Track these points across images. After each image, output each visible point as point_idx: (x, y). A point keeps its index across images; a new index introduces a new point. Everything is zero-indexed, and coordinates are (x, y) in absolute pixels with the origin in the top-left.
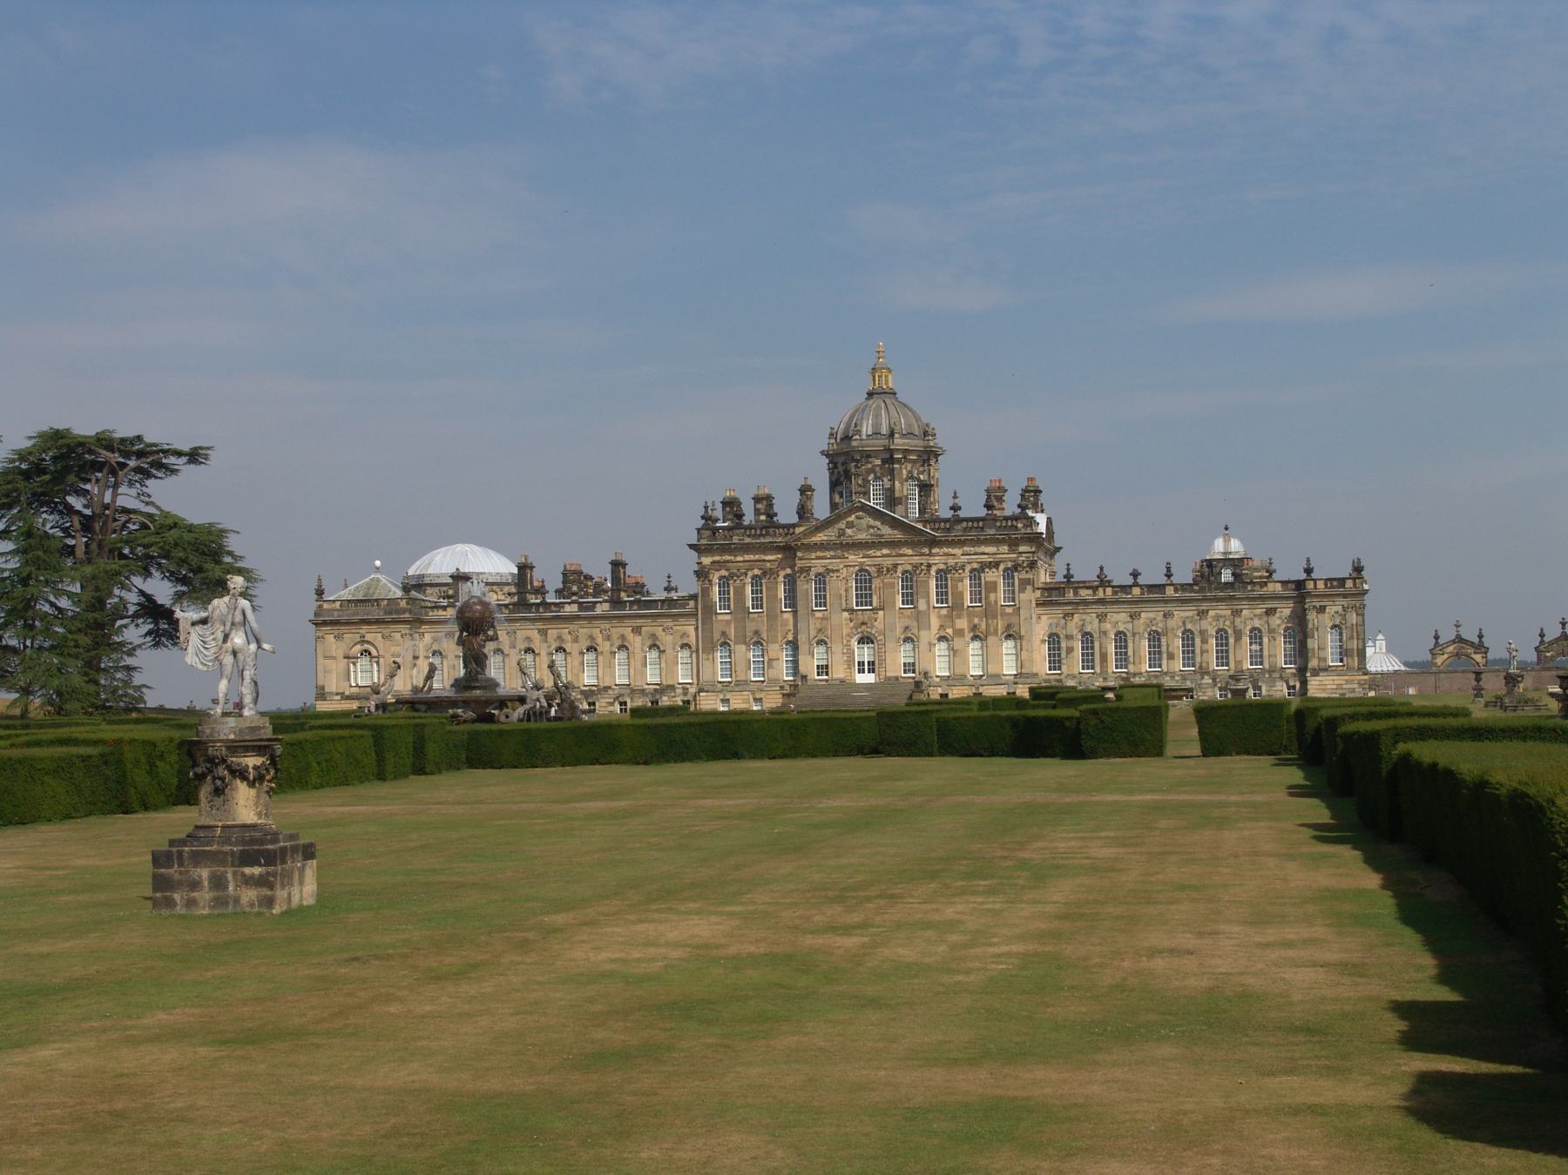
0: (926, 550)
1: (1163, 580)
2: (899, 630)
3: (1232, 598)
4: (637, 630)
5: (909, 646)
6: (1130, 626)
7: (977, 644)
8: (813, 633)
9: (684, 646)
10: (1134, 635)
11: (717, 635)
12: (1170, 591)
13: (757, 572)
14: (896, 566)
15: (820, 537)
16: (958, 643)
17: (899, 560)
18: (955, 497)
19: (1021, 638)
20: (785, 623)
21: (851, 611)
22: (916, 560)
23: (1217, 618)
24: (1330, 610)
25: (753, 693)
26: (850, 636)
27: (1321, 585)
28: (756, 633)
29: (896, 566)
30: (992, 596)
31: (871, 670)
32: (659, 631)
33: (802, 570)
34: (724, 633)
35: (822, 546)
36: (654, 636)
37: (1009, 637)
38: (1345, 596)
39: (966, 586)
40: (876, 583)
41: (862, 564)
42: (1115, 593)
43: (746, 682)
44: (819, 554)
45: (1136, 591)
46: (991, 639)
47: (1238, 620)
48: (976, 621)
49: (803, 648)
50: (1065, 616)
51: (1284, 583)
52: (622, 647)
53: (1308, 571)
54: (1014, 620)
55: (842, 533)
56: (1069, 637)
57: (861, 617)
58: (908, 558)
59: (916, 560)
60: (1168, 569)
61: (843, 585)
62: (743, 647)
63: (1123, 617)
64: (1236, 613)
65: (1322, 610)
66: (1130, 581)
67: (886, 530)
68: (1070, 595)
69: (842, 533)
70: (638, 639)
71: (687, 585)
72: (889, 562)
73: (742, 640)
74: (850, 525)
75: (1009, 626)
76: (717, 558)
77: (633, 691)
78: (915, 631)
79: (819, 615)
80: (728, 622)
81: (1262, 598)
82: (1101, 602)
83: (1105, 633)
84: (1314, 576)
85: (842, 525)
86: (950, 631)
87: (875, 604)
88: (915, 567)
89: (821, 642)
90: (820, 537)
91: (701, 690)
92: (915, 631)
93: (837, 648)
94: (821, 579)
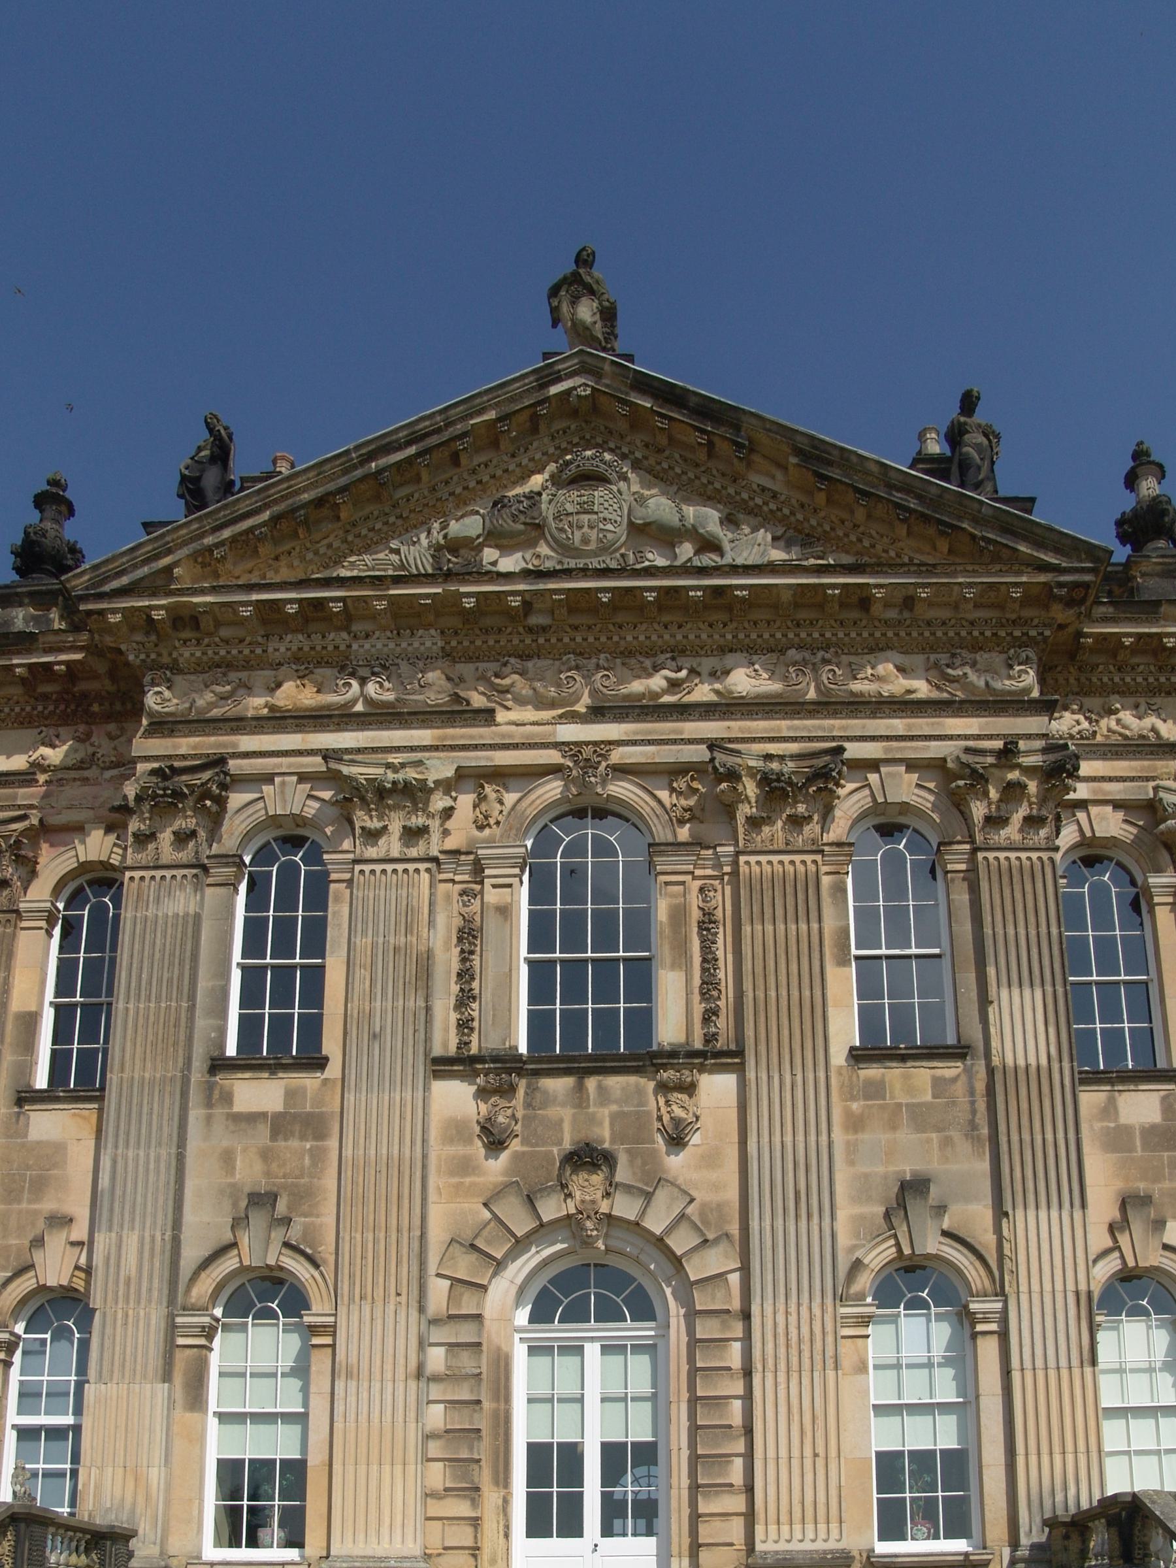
2: (851, 1213)
5: (920, 1334)
26: (482, 1252)
29: (824, 773)
40: (676, 895)
44: (295, 694)
49: (129, 1324)
55: (457, 561)
61: (438, 923)
79: (259, 1094)
85: (469, 526)
87: (672, 1024)
89: (267, 1293)
92: (976, 1215)
93: (378, 1333)
94: (291, 873)
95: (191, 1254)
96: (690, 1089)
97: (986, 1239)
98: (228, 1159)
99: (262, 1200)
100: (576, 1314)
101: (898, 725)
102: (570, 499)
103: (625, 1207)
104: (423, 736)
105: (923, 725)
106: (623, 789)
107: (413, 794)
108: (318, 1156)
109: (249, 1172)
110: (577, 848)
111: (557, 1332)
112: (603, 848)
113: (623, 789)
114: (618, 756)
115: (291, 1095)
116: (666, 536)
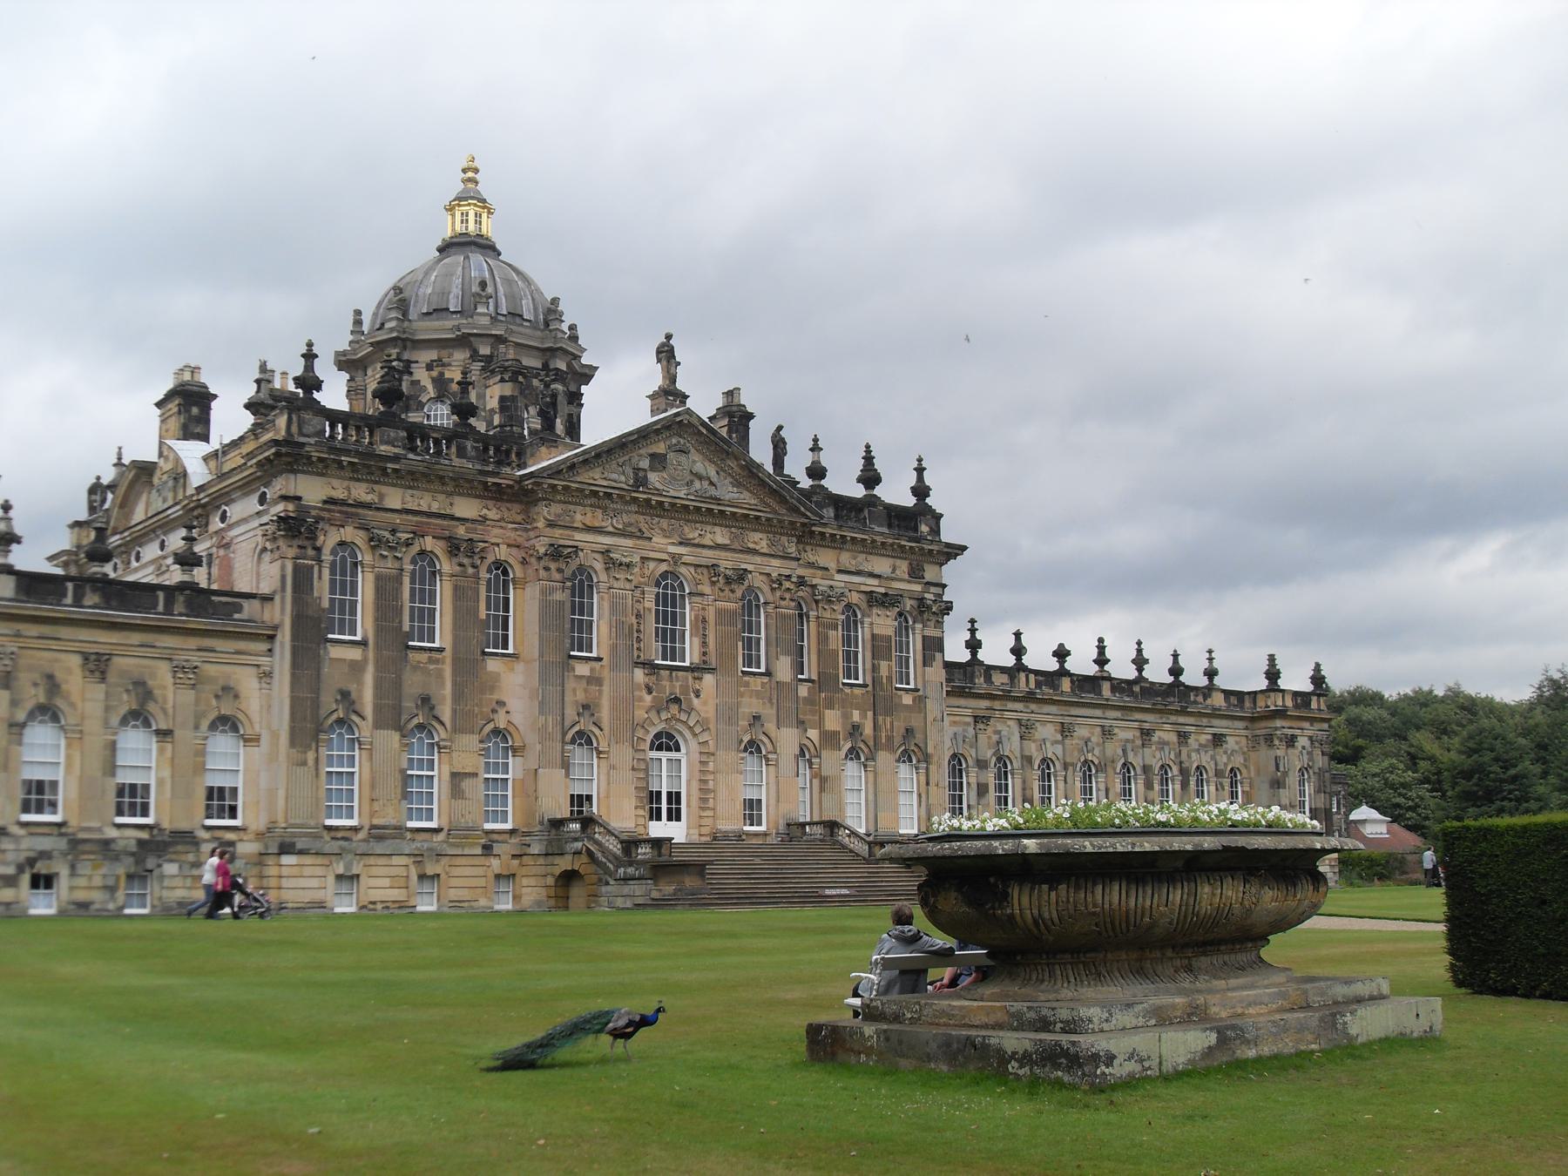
0: (792, 549)
1: (1092, 670)
3: (1183, 712)
4: (97, 665)
5: (751, 763)
6: (1059, 749)
7: (852, 768)
8: (571, 713)
9: (227, 723)
10: (1066, 766)
11: (328, 701)
12: (1106, 686)
13: (429, 543)
14: (742, 575)
15: (595, 477)
16: (831, 760)
17: (749, 562)
18: (816, 448)
19: (927, 758)
20: (492, 684)
21: (650, 667)
22: (776, 567)
23: (1163, 744)
24: (1303, 741)
25: (418, 857)
27: (1289, 703)
28: (426, 701)
30: (884, 664)
31: (674, 815)
32: (162, 677)
33: (556, 553)
34: (345, 695)
35: (600, 498)
36: (143, 690)
37: (906, 757)
38: (1312, 720)
39: (835, 638)
41: (676, 558)
42: (1038, 684)
43: (399, 831)
45: (1066, 684)
46: (884, 758)
47: (1184, 751)
48: (856, 716)
50: (976, 719)
51: (1228, 694)
52: (47, 712)
53: (1273, 675)
54: (916, 722)
56: (982, 764)
57: (669, 686)
58: (765, 562)
59: (776, 567)
60: (1101, 648)
62: (396, 736)
63: (1047, 732)
64: (1183, 737)
65: (1291, 741)
66: (1052, 665)
67: (727, 491)
68: (980, 681)
69: (640, 481)
70: (98, 691)
71: (248, 560)
72: (727, 562)
73: (389, 717)
74: (658, 461)
75: (909, 731)
76: (339, 494)
77: (75, 843)
78: (770, 727)
79: (582, 669)
80: (356, 668)
81: (1215, 714)
82: (1029, 697)
83: (1028, 760)
84: (1283, 683)
86: (813, 734)
88: (777, 583)
89: (583, 738)
90: (595, 477)
91: (286, 849)
94: (581, 585)
95: (567, 723)
96: (700, 679)
97: (773, 735)
98: (574, 690)
99: (586, 707)
100: (659, 748)
101: (758, 559)
102: (671, 456)
103: (683, 717)
104: (629, 542)
105: (766, 559)
106: (683, 570)
107: (628, 565)
108: (600, 692)
109: (581, 696)
110: (666, 587)
111: (655, 754)
112: (673, 588)
113: (683, 570)
114: (686, 559)
115: (592, 670)
116: (700, 478)
